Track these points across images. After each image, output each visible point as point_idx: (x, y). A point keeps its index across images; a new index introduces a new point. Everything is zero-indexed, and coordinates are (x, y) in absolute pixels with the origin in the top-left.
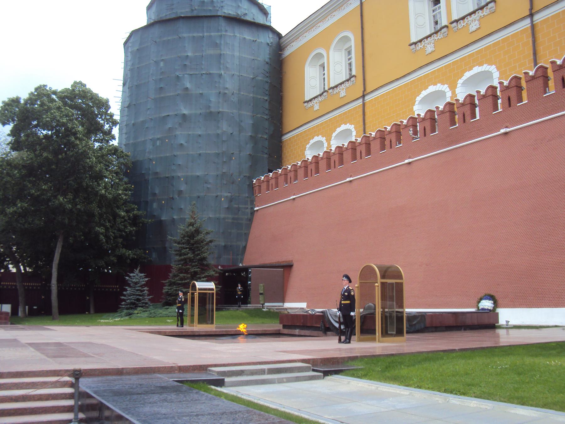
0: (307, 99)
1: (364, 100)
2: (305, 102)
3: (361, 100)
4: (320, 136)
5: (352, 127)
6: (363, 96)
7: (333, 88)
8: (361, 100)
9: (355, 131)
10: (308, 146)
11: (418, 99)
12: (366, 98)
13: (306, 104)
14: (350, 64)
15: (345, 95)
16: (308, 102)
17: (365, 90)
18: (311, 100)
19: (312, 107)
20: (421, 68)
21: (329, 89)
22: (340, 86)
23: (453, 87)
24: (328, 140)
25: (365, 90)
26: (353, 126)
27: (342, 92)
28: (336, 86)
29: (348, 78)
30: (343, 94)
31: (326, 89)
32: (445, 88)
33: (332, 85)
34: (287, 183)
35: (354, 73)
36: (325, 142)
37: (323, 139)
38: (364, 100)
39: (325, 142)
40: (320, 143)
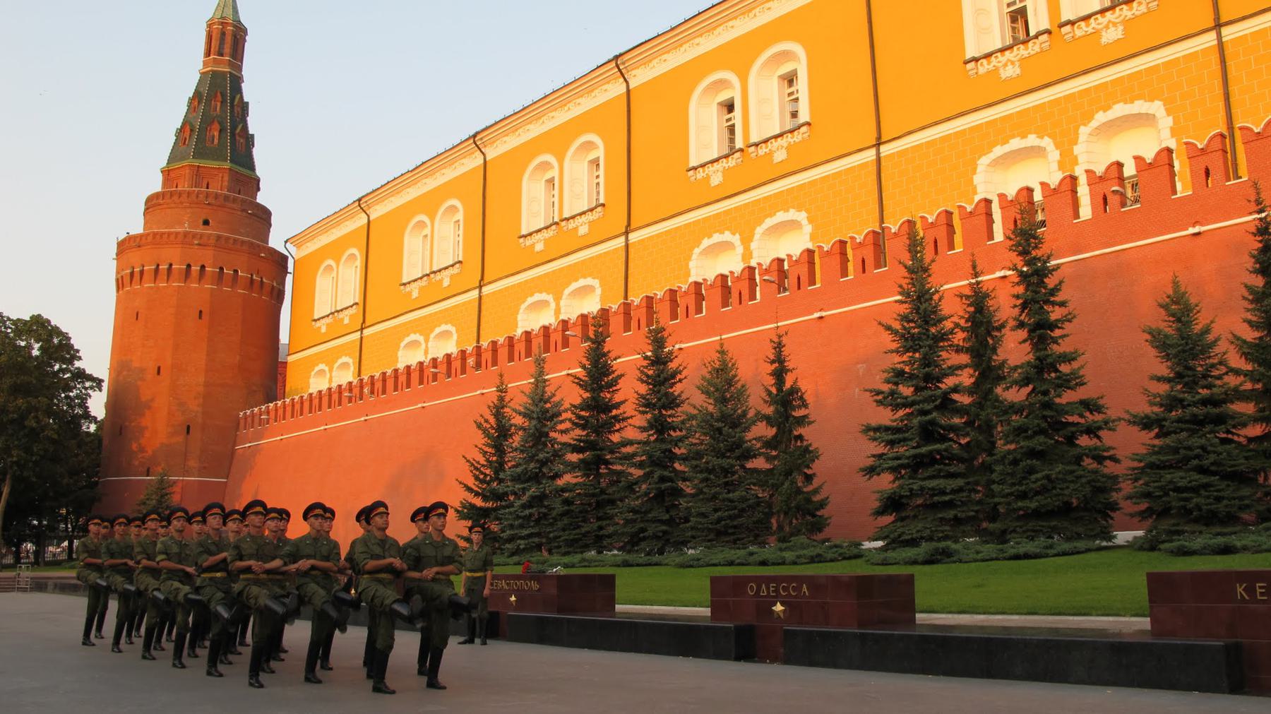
0: (316, 317)
1: (362, 333)
2: (315, 320)
3: (359, 333)
6: (362, 329)
7: (338, 311)
8: (359, 333)
10: (313, 373)
11: (402, 345)
12: (365, 331)
13: (314, 323)
17: (364, 322)
18: (319, 319)
20: (406, 313)
25: (364, 322)
27: (346, 317)
28: (342, 310)
30: (346, 321)
33: (338, 309)
36: (328, 372)
37: (326, 369)
38: (362, 333)
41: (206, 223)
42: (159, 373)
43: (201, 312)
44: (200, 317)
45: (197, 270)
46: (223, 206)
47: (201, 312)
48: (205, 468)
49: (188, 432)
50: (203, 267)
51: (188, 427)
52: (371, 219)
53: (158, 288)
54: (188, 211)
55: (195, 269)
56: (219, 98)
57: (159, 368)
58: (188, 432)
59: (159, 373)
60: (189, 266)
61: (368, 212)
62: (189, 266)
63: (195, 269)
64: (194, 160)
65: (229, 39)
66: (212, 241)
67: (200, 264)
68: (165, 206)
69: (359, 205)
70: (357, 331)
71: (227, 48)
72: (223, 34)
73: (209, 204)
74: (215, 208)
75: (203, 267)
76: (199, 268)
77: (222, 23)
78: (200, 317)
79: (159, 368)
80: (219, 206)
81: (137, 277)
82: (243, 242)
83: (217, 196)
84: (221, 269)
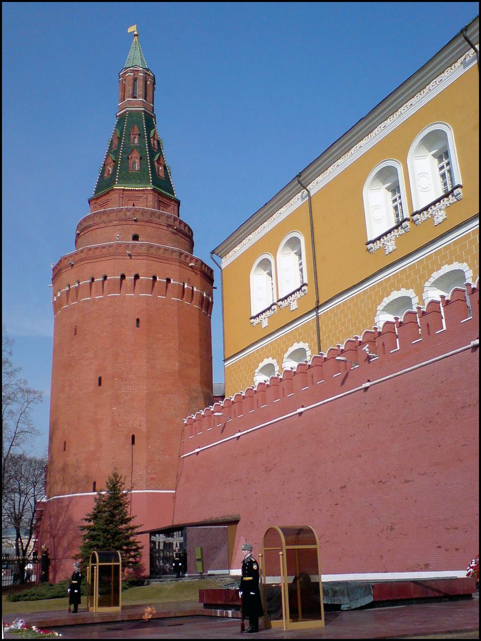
0: (254, 314)
2: (252, 318)
4: (270, 358)
5: (305, 346)
6: (318, 308)
7: (282, 300)
9: (310, 351)
13: (253, 320)
14: (301, 270)
15: (297, 307)
16: (254, 318)
17: (318, 302)
19: (260, 324)
21: (278, 301)
22: (290, 297)
23: (420, 292)
24: (280, 362)
25: (318, 302)
26: (307, 344)
29: (299, 286)
31: (275, 301)
32: (410, 293)
34: (230, 418)
35: (306, 281)
36: (276, 365)
37: (274, 362)
39: (276, 365)
40: (270, 367)
41: (136, 238)
42: (100, 384)
43: (138, 320)
44: (138, 326)
45: (130, 280)
46: (150, 222)
47: (138, 320)
48: (153, 479)
49: (133, 442)
50: (137, 277)
51: (133, 437)
52: (312, 194)
53: (94, 301)
54: (118, 227)
55: (130, 278)
56: (137, 131)
57: (100, 379)
58: (133, 442)
59: (100, 384)
60: (123, 277)
61: (308, 188)
62: (123, 277)
63: (130, 278)
64: (118, 185)
65: (140, 84)
66: (143, 250)
67: (134, 273)
68: (96, 227)
69: (299, 182)
70: (310, 312)
71: (140, 91)
72: (135, 80)
73: (136, 221)
74: (143, 223)
75: (137, 277)
76: (133, 277)
77: (134, 71)
78: (138, 326)
79: (100, 379)
80: (147, 222)
81: (72, 294)
82: (173, 251)
83: (144, 212)
84: (155, 278)
